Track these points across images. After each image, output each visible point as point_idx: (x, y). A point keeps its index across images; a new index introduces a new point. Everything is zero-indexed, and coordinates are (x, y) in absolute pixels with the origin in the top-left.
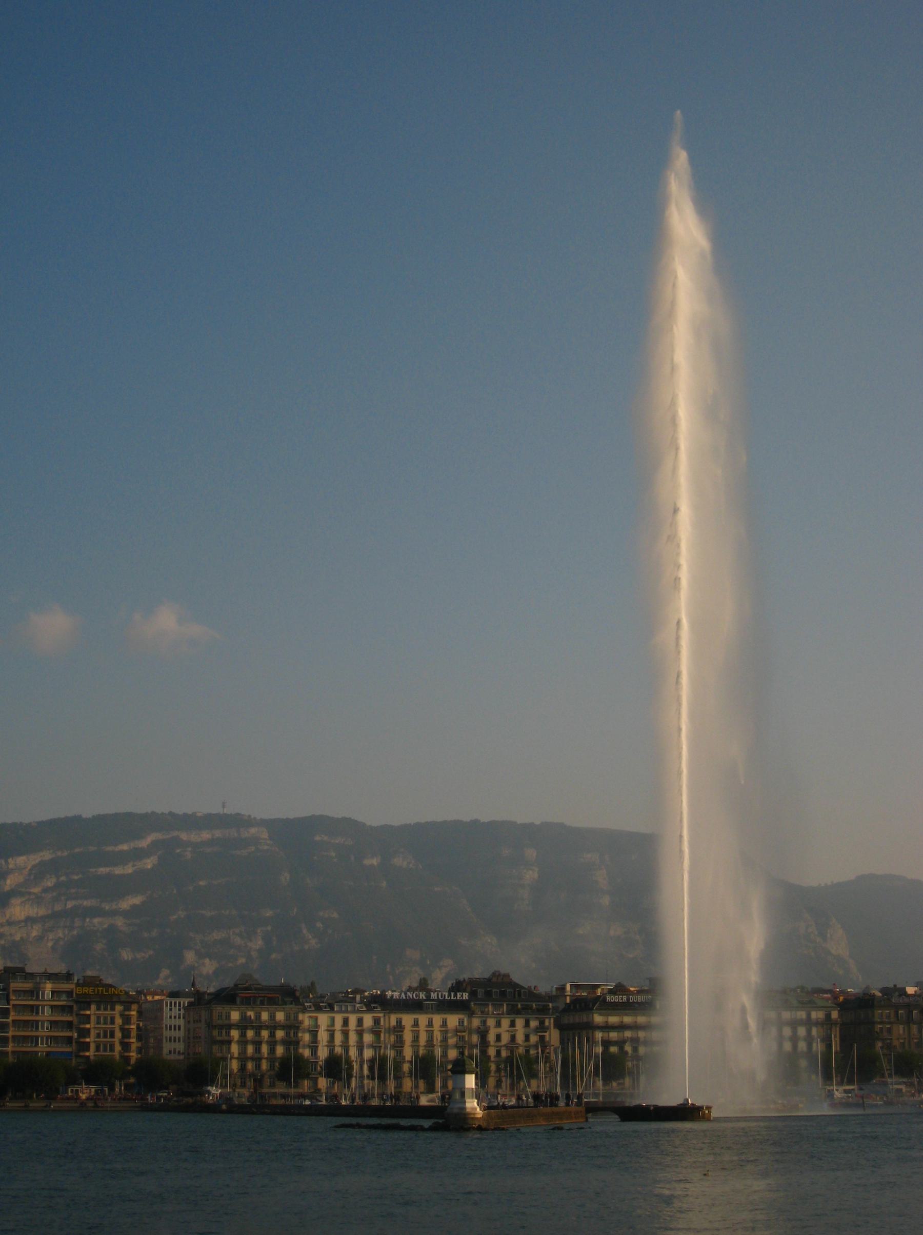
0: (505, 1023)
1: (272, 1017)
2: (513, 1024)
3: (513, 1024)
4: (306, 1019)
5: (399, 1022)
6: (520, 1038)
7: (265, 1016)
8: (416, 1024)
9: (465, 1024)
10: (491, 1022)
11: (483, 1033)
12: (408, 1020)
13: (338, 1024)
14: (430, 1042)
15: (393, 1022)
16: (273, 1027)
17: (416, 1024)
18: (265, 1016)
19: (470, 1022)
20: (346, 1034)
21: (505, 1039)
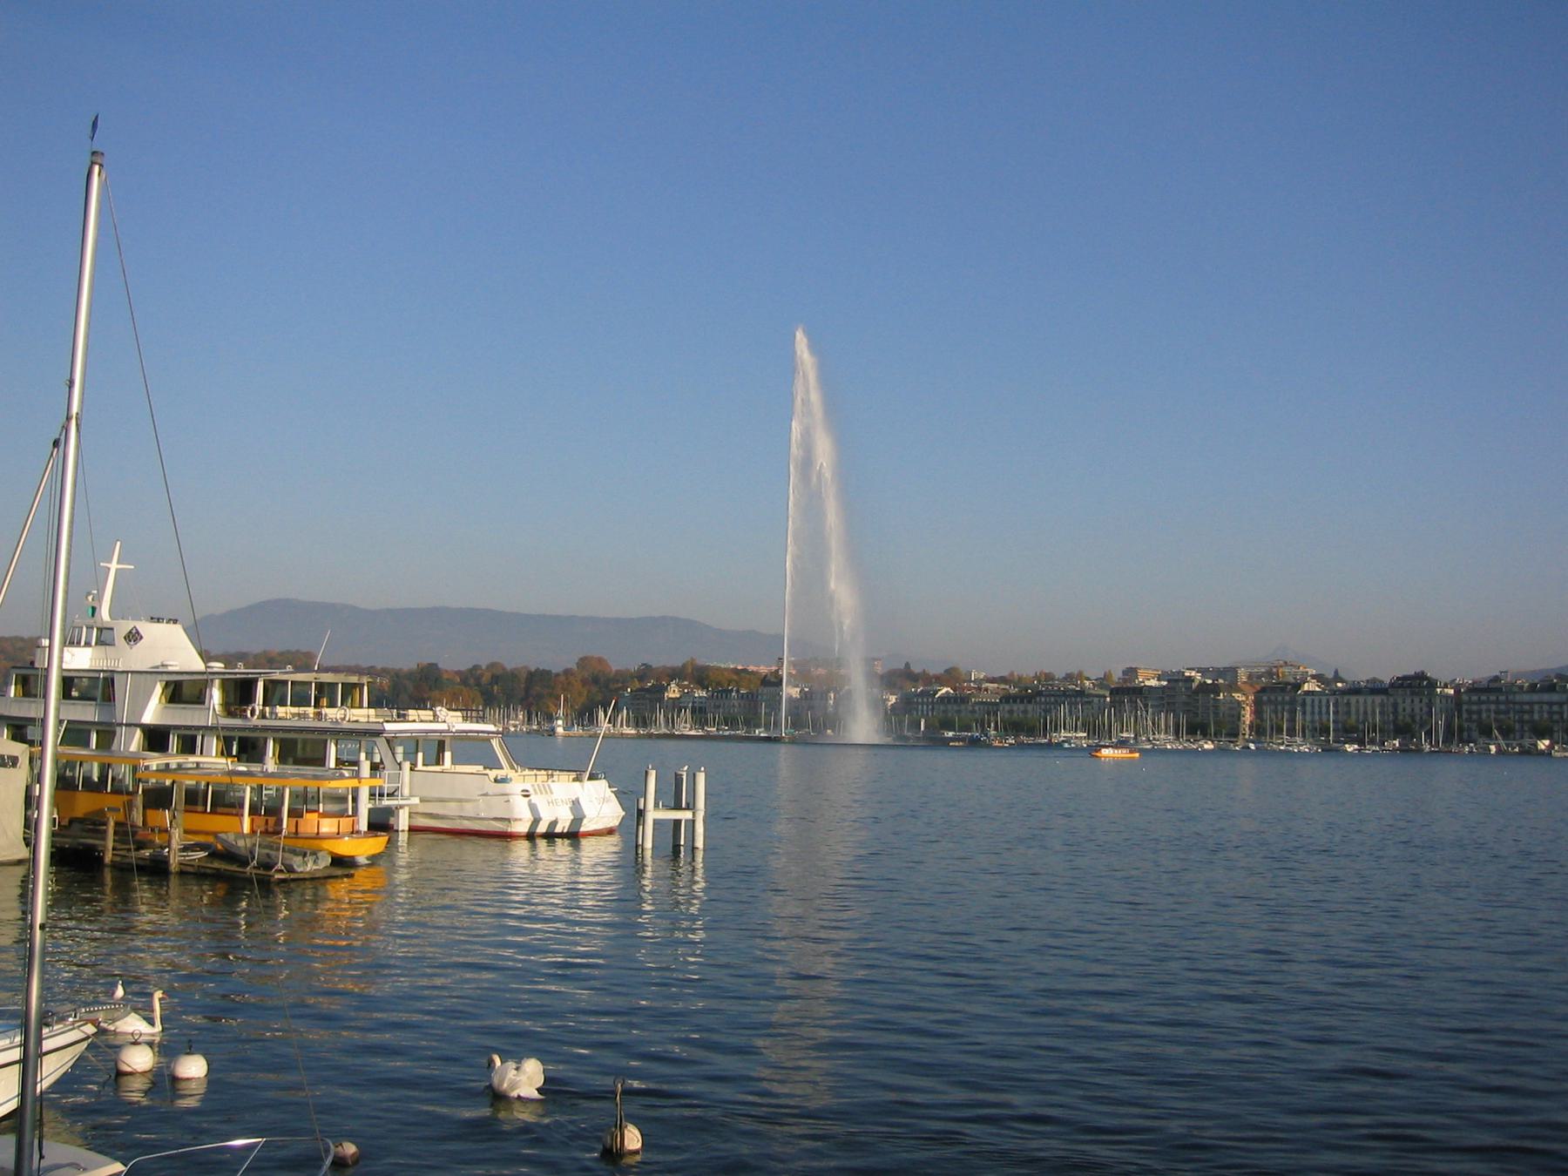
0: (1408, 701)
1: (1283, 699)
2: (1412, 701)
3: (1412, 701)
4: (1300, 699)
5: (1348, 700)
6: (1417, 710)
7: (1280, 698)
8: (1358, 702)
9: (1385, 701)
10: (1400, 701)
11: (1395, 705)
12: (1353, 699)
13: (1316, 703)
14: (1365, 713)
15: (1345, 701)
16: (1283, 703)
17: (1358, 702)
18: (1280, 698)
19: (1388, 700)
20: (1320, 707)
21: (1408, 710)
